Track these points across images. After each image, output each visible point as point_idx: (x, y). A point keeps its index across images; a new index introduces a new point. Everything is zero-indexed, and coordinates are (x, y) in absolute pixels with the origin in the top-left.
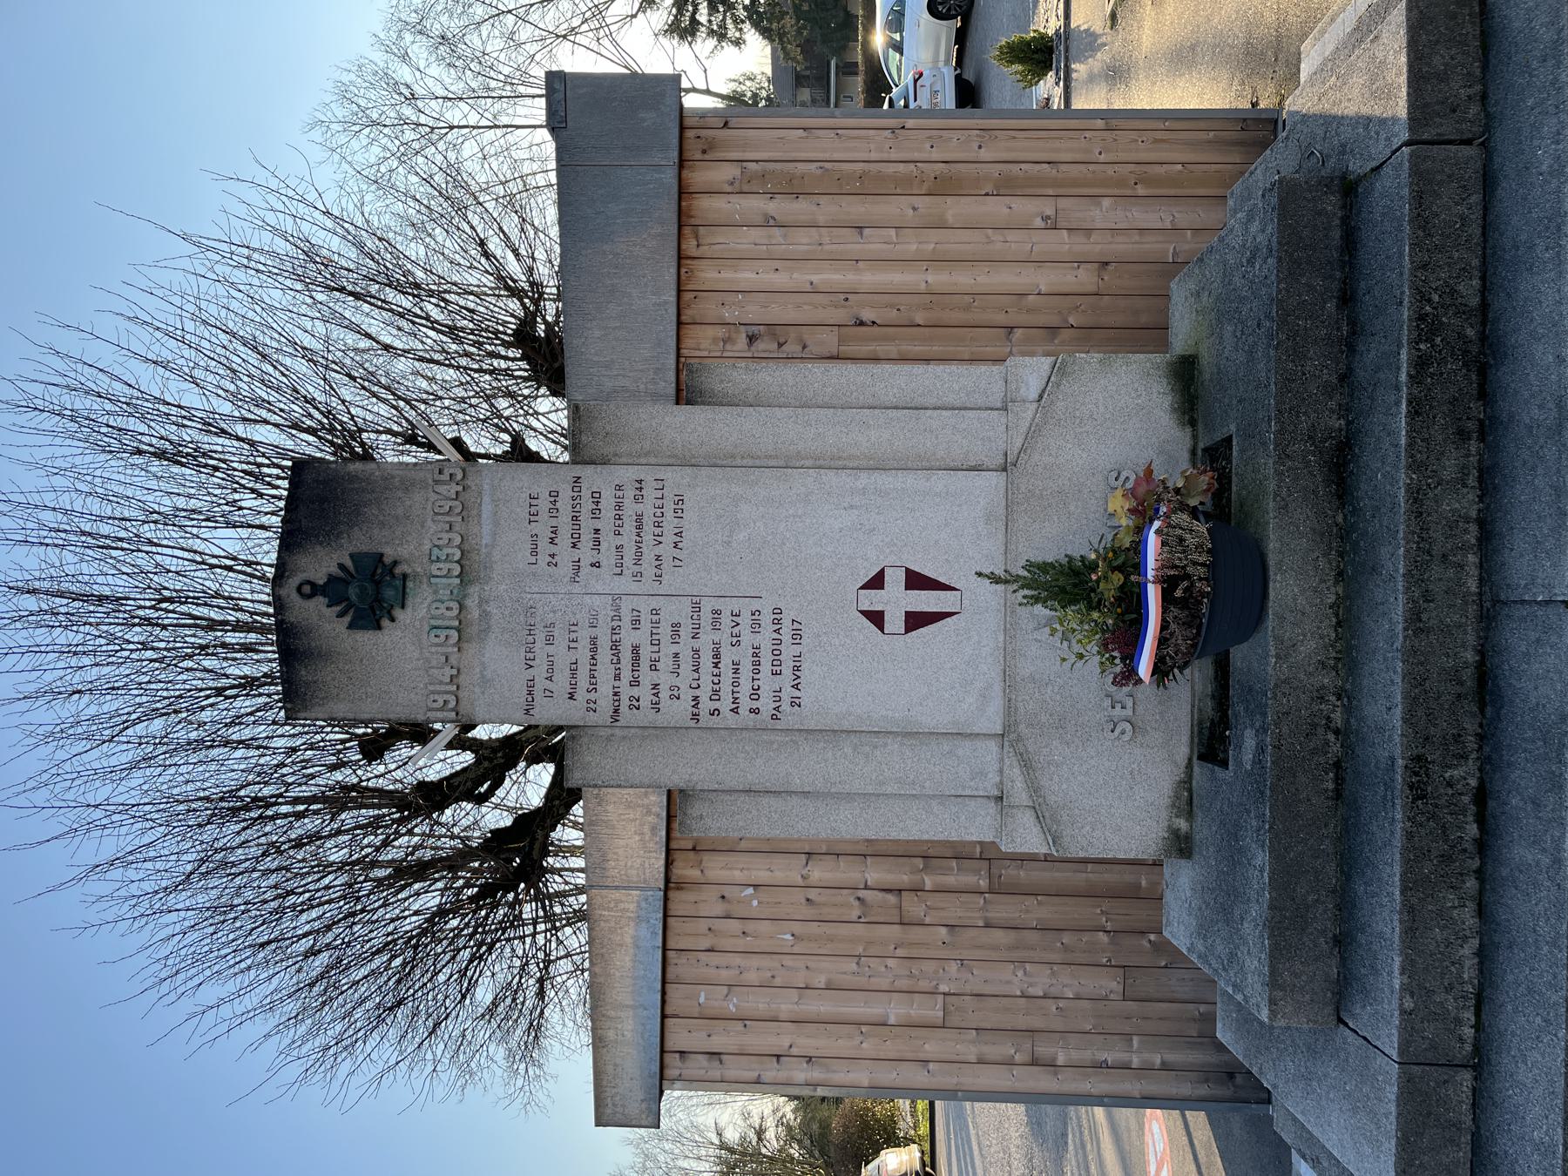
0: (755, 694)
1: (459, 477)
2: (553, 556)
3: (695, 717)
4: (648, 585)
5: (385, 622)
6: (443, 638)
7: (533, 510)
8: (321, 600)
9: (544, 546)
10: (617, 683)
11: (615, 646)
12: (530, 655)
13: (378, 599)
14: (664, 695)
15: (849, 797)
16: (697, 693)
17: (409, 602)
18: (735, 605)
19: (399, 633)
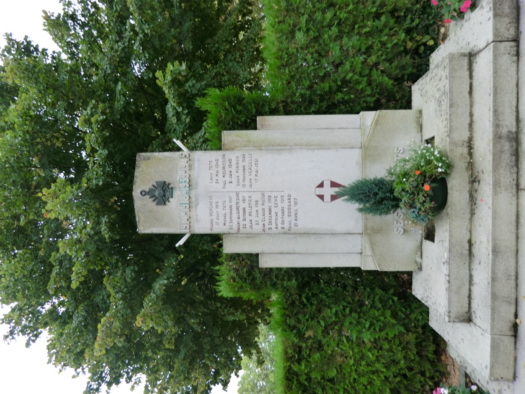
0: (283, 222)
2: (217, 180)
3: (264, 230)
4: (247, 188)
5: (167, 203)
9: (214, 177)
11: (238, 208)
13: (164, 196)
14: (254, 223)
15: (314, 254)
16: (264, 222)
17: (174, 195)
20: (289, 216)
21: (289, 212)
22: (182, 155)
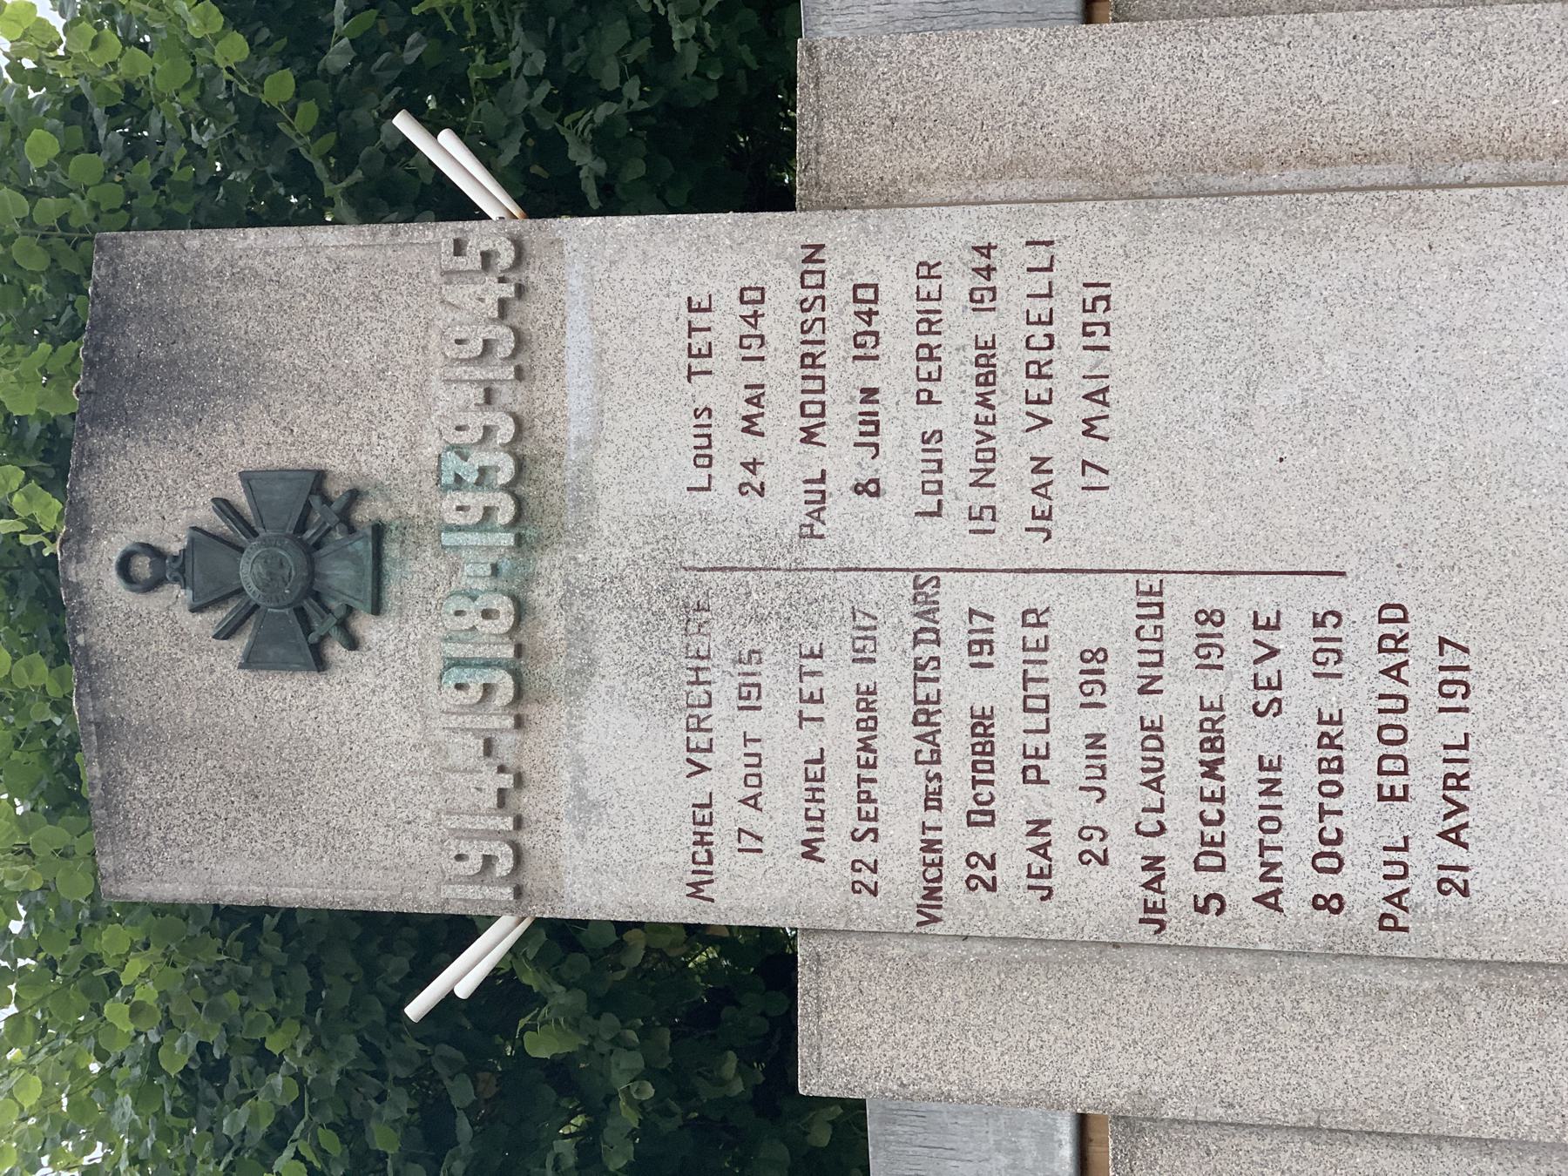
0: (1329, 854)
1: (506, 257)
2: (752, 466)
3: (1153, 915)
5: (336, 651)
6: (475, 692)
7: (699, 340)
8: (176, 595)
9: (729, 442)
10: (932, 818)
11: (925, 715)
12: (700, 739)
13: (314, 593)
14: (1064, 849)
16: (1157, 846)
17: (392, 589)
18: (1264, 596)
19: (367, 677)
22: (459, 248)
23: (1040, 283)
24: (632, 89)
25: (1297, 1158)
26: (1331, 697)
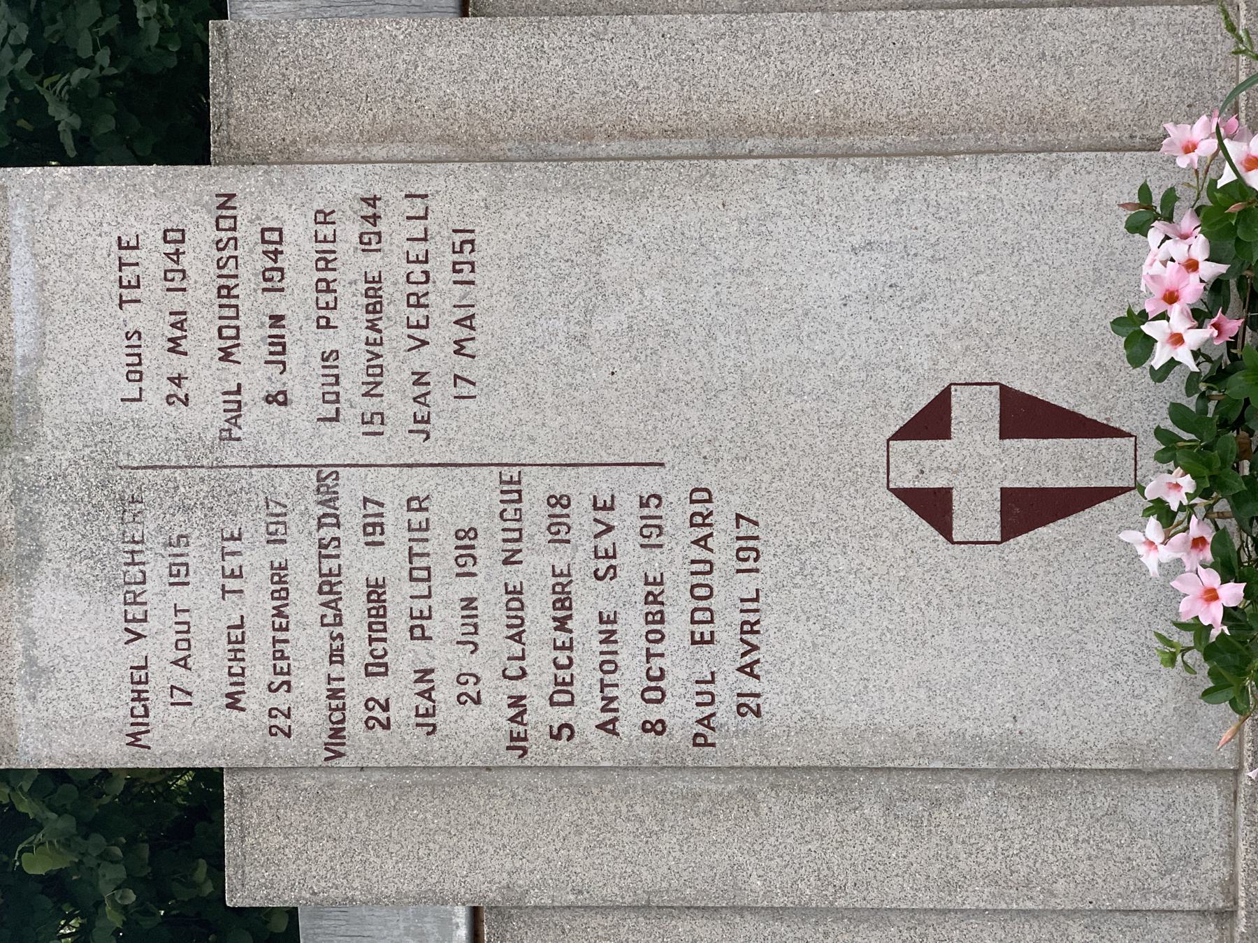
0: (654, 689)
2: (177, 380)
3: (518, 743)
10: (336, 670)
11: (329, 585)
12: (136, 611)
14: (445, 693)
16: (520, 688)
18: (601, 483)
20: (699, 641)
21: (702, 614)
23: (417, 229)
24: (104, 57)
25: (632, 931)
26: (655, 563)
